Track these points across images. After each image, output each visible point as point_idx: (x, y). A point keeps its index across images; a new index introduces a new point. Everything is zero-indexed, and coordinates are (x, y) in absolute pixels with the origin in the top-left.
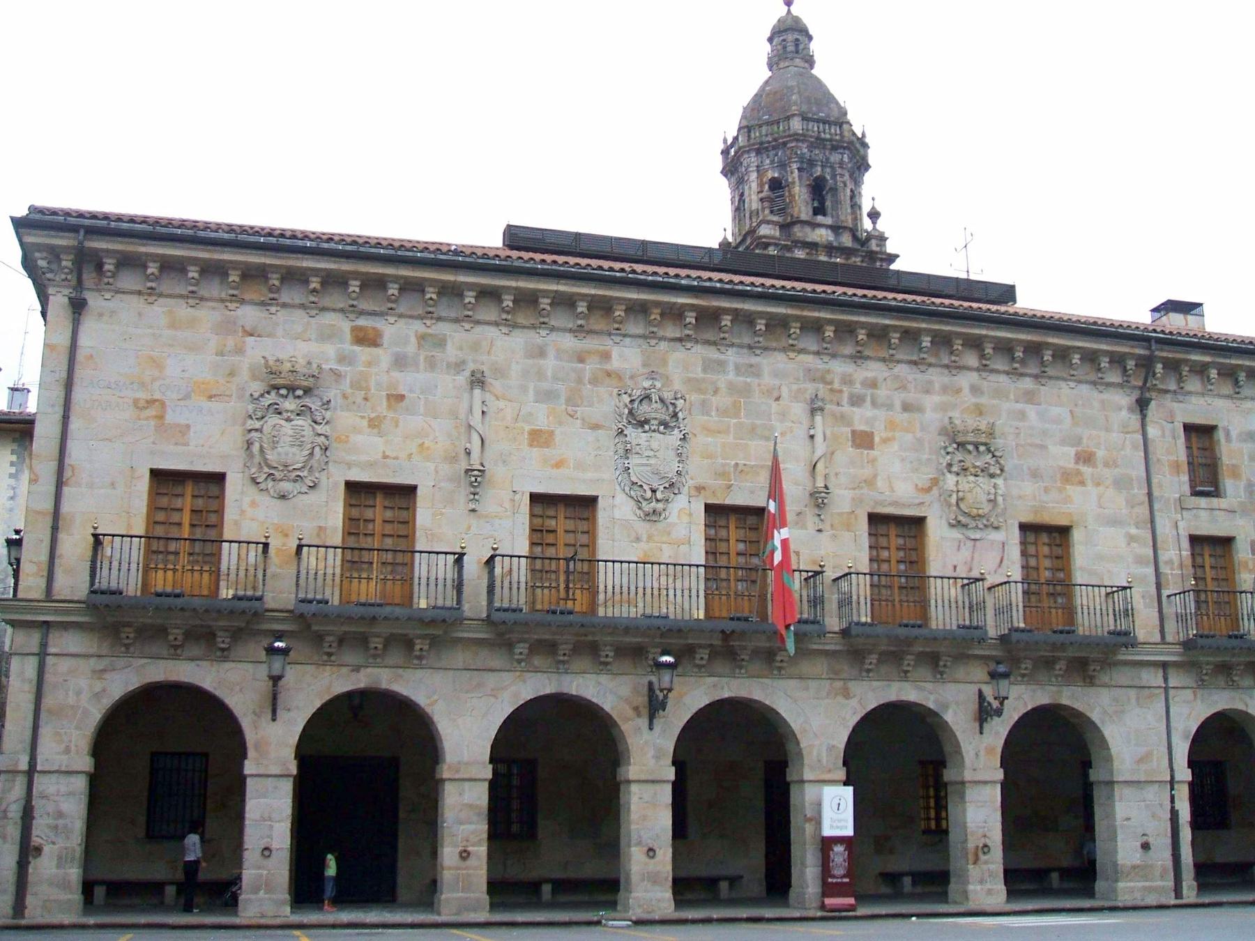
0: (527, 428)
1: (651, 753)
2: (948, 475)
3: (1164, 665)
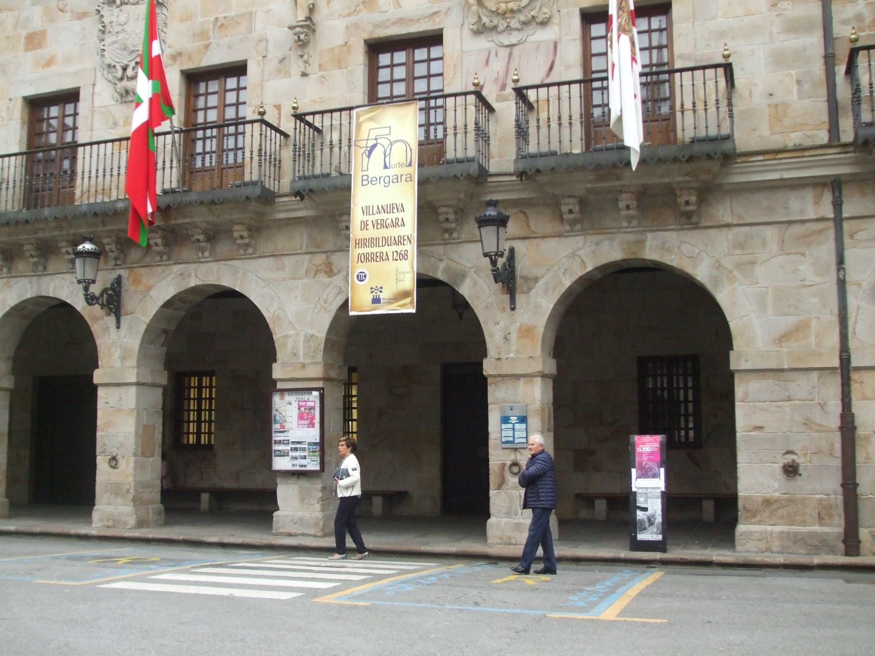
0: (24, 33)
1: (117, 354)
3: (836, 185)
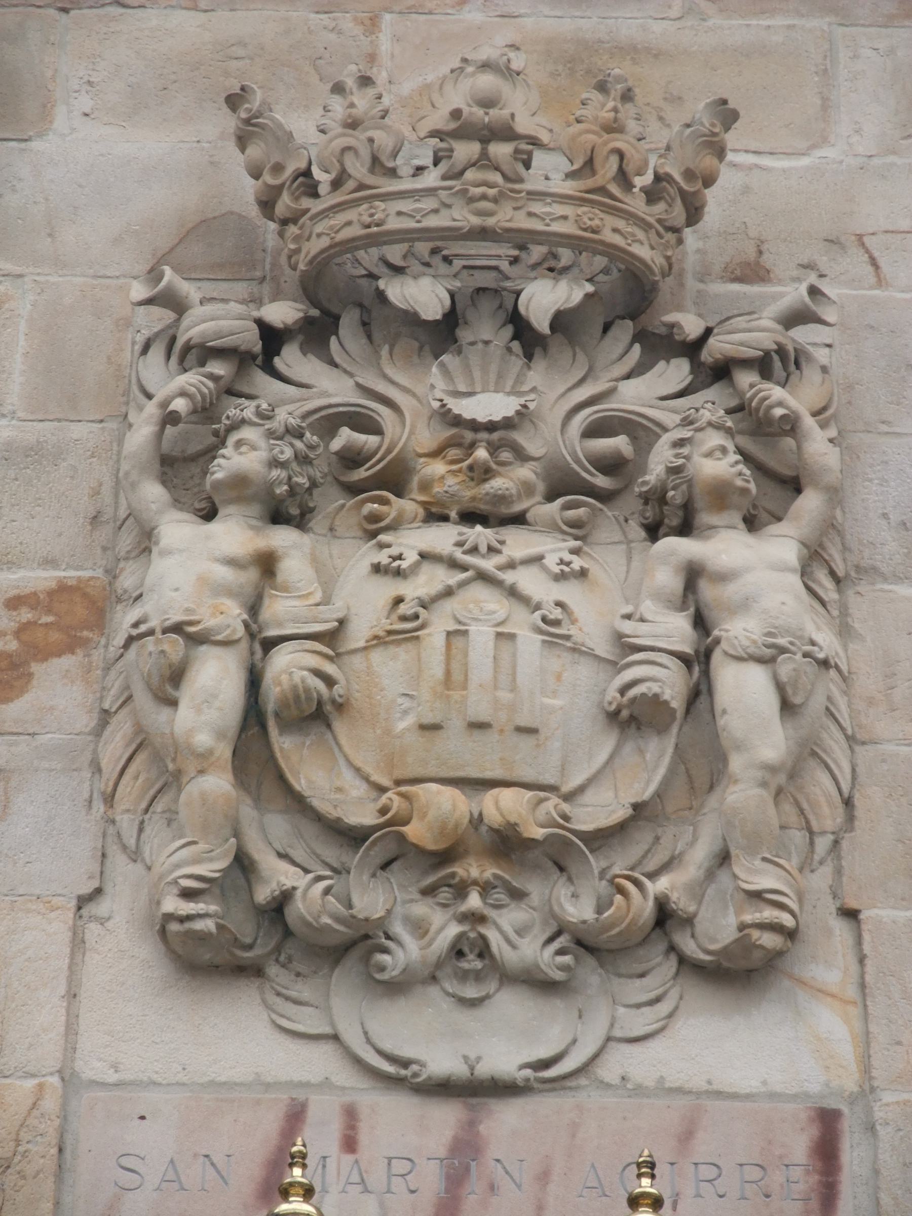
2: (177, 530)
